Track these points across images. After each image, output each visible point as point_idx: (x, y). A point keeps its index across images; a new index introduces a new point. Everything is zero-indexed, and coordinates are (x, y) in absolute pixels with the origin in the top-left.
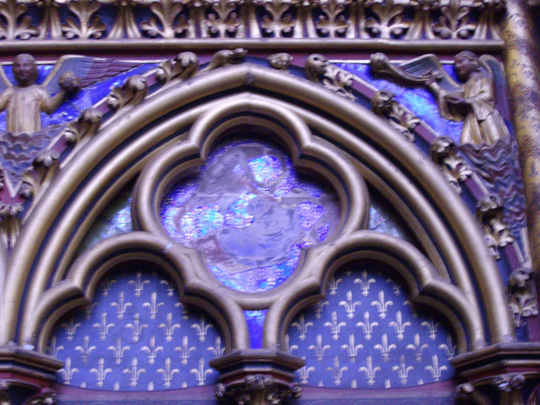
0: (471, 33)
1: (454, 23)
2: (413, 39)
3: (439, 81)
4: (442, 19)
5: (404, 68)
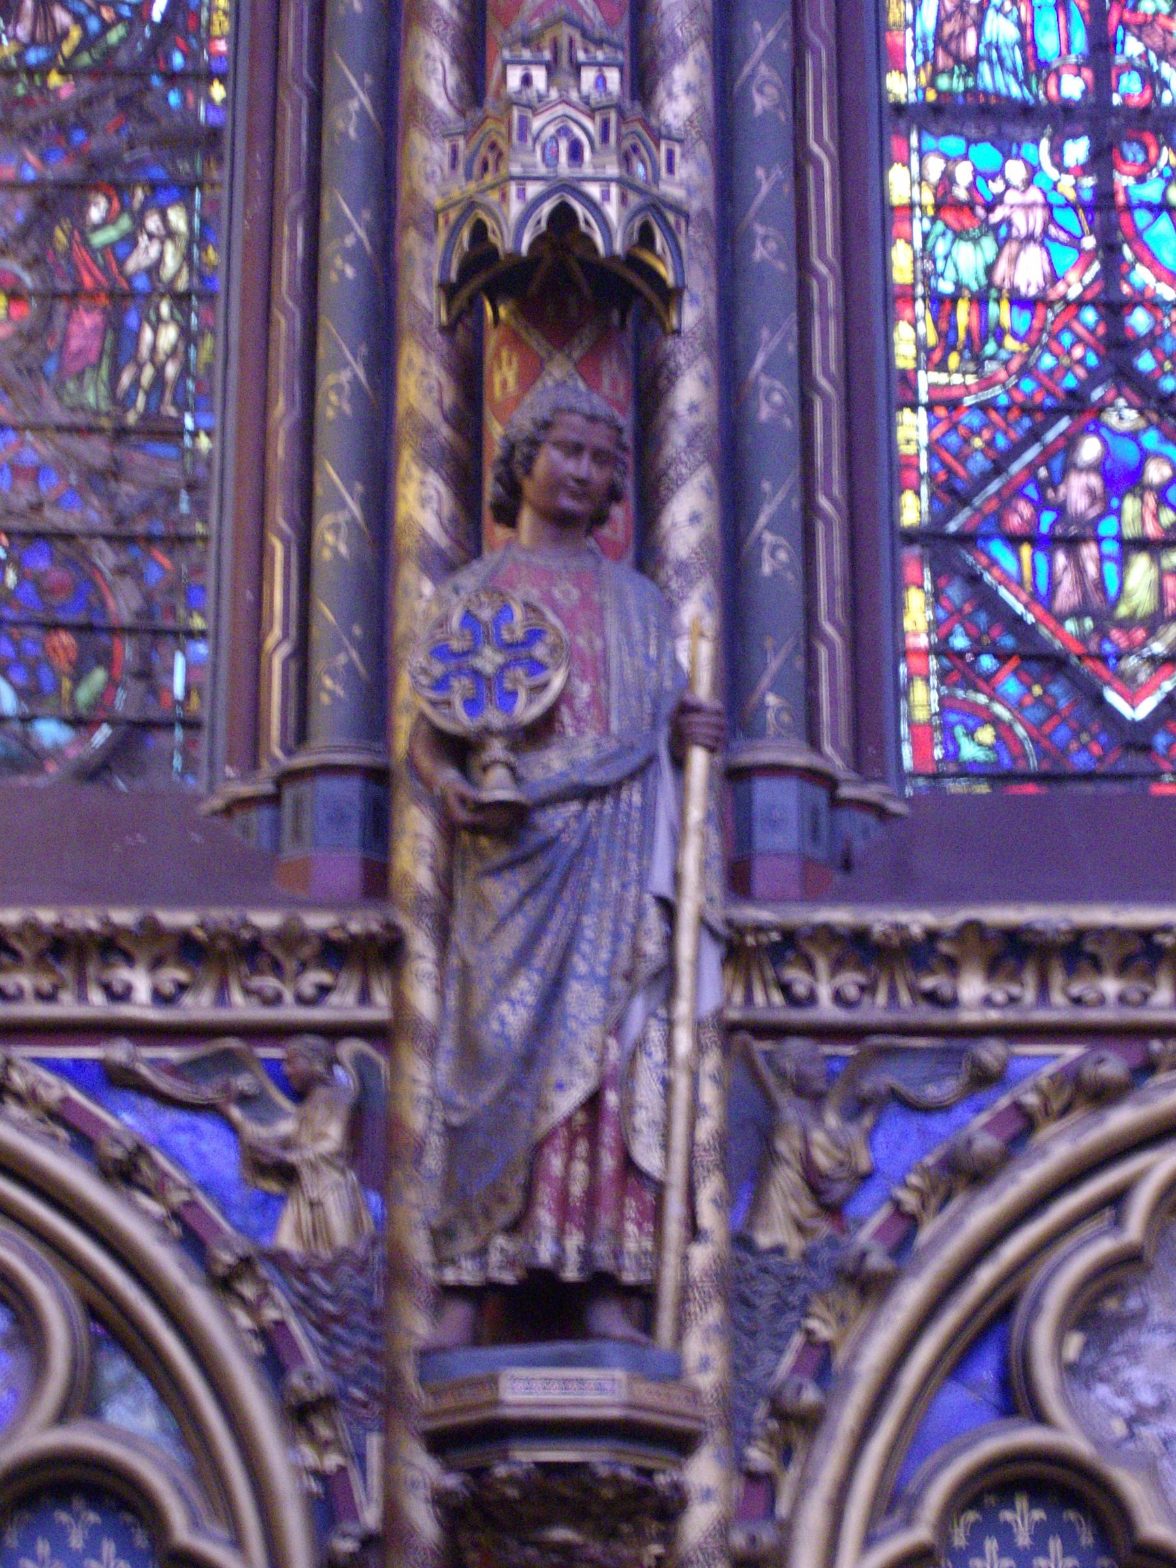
0: (324, 990)
1: (290, 965)
2: (199, 1006)
3: (244, 1100)
4: (263, 962)
5: (175, 1070)
